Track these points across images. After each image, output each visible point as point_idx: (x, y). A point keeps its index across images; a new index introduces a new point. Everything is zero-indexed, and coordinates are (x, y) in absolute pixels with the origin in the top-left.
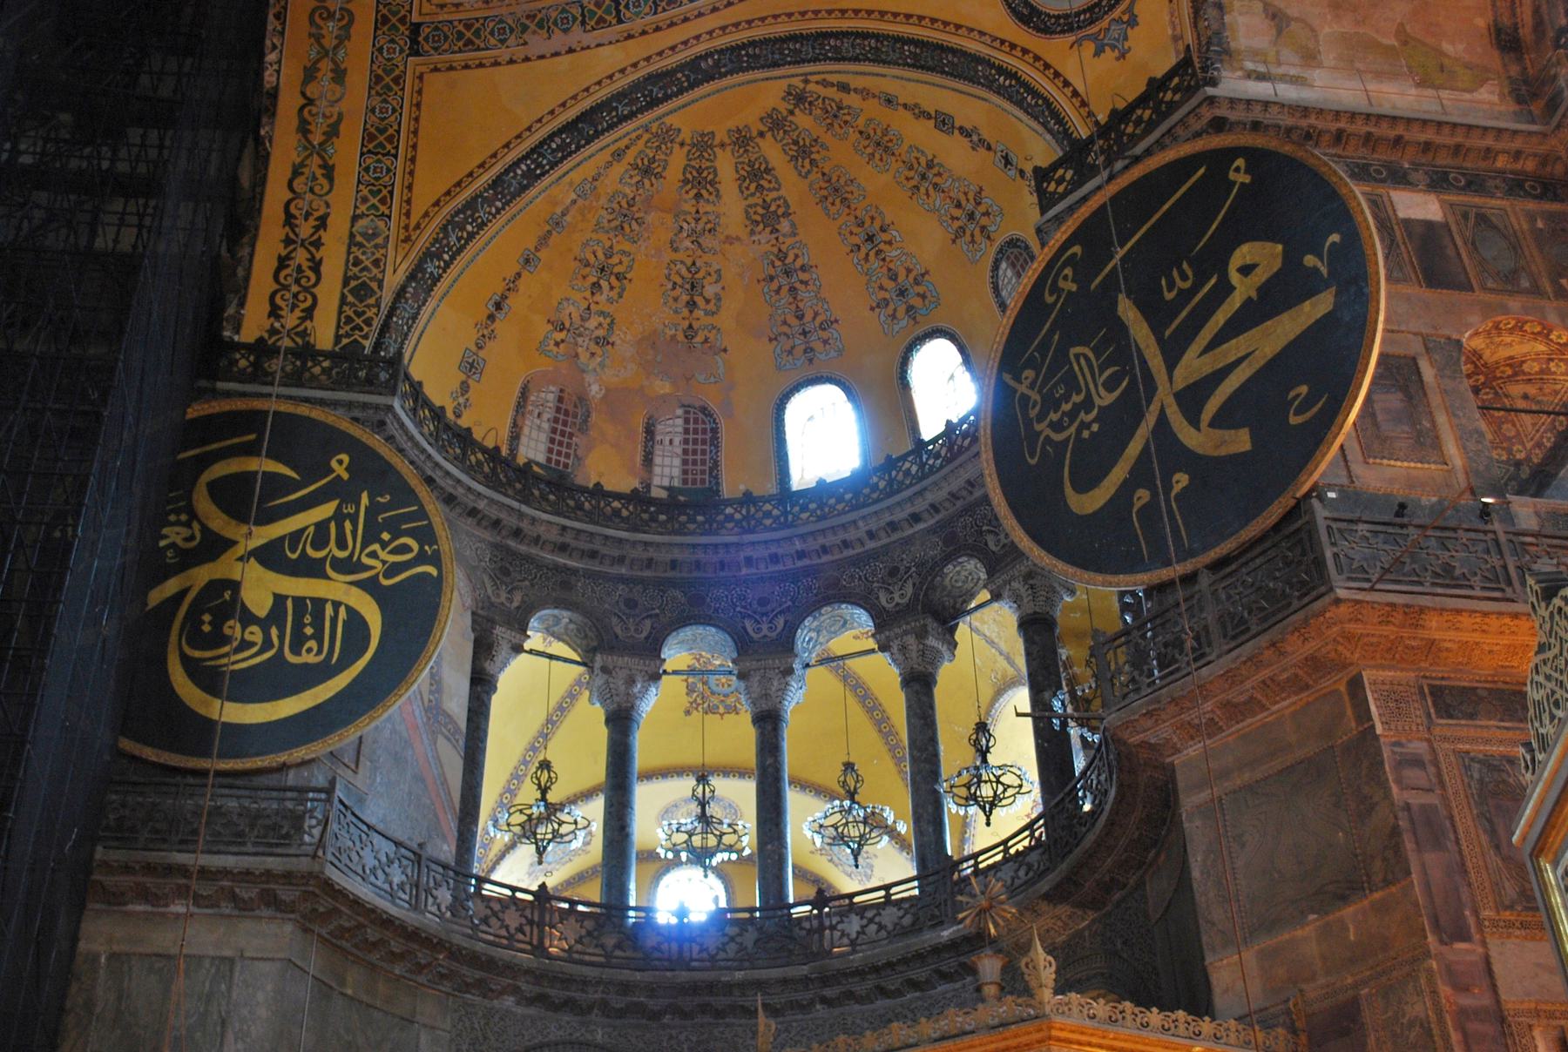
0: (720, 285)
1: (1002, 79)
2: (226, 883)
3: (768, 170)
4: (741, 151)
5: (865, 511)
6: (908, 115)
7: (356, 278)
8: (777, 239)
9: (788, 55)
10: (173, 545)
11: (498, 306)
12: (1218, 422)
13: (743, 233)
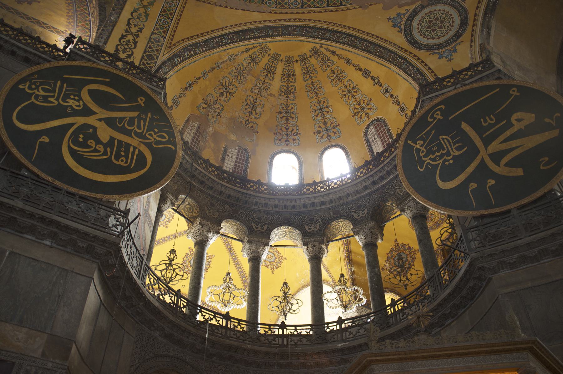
0: (262, 109)
1: (400, 60)
2: (75, 237)
3: (293, 75)
4: (288, 65)
5: (304, 196)
6: (353, 68)
7: (149, 52)
8: (287, 100)
9: (320, 35)
10: (71, 106)
11: (190, 85)
12: (508, 165)
13: (276, 94)
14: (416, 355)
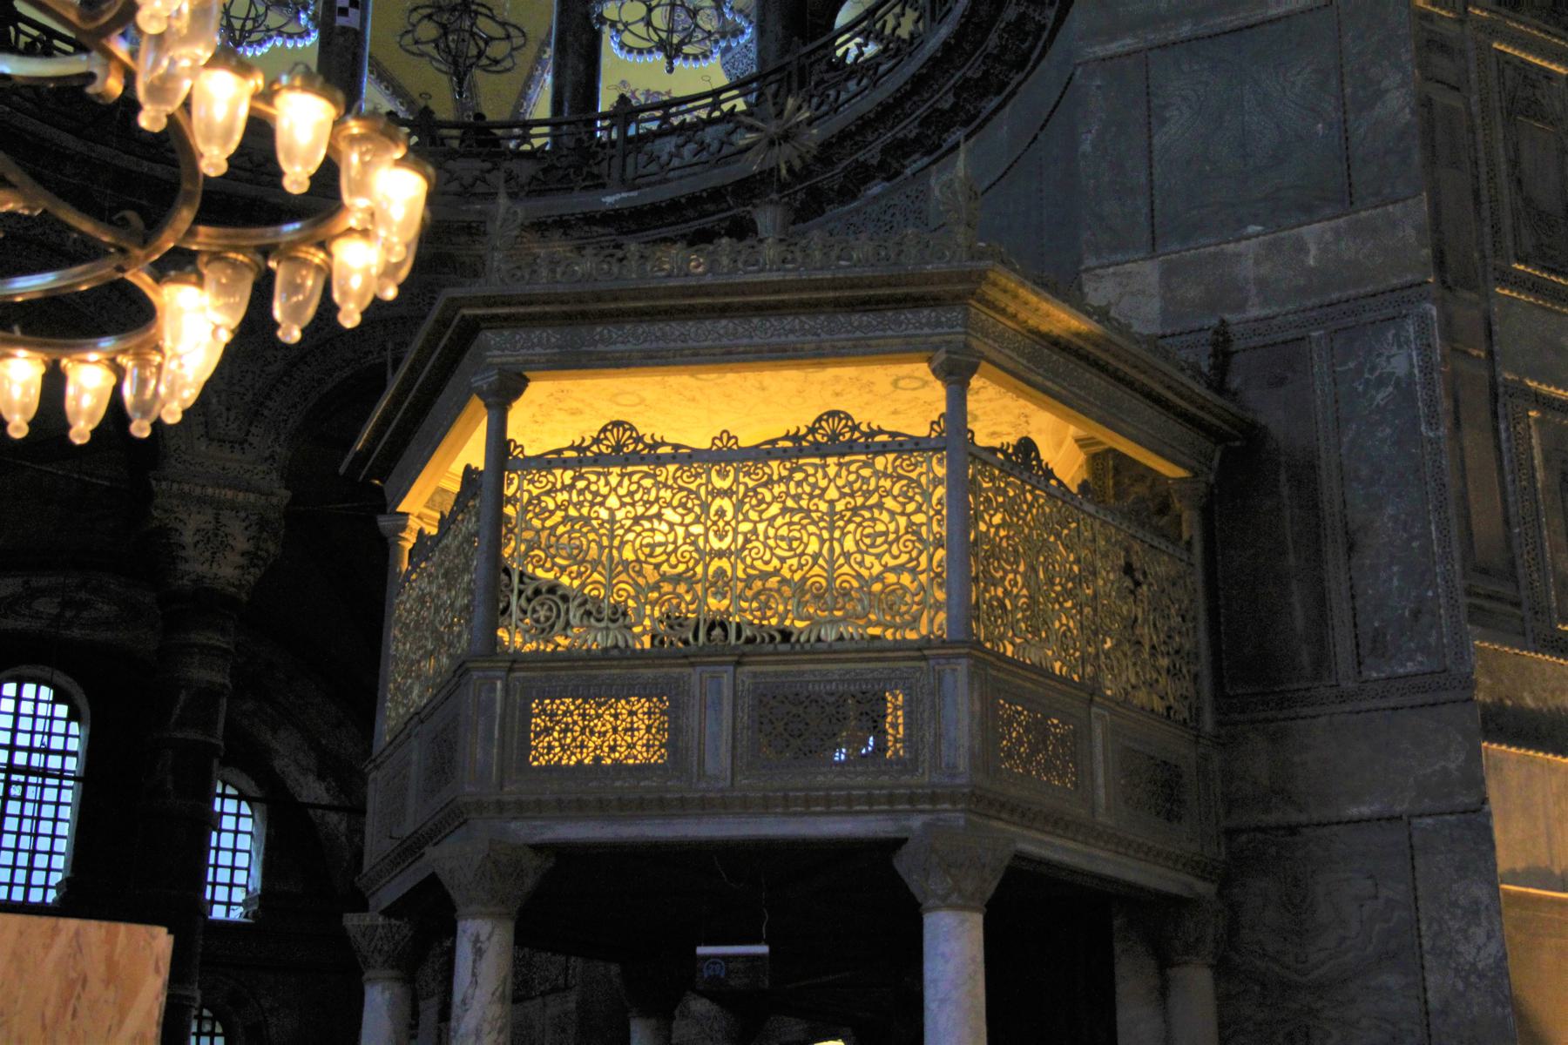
14: (613, 306)
